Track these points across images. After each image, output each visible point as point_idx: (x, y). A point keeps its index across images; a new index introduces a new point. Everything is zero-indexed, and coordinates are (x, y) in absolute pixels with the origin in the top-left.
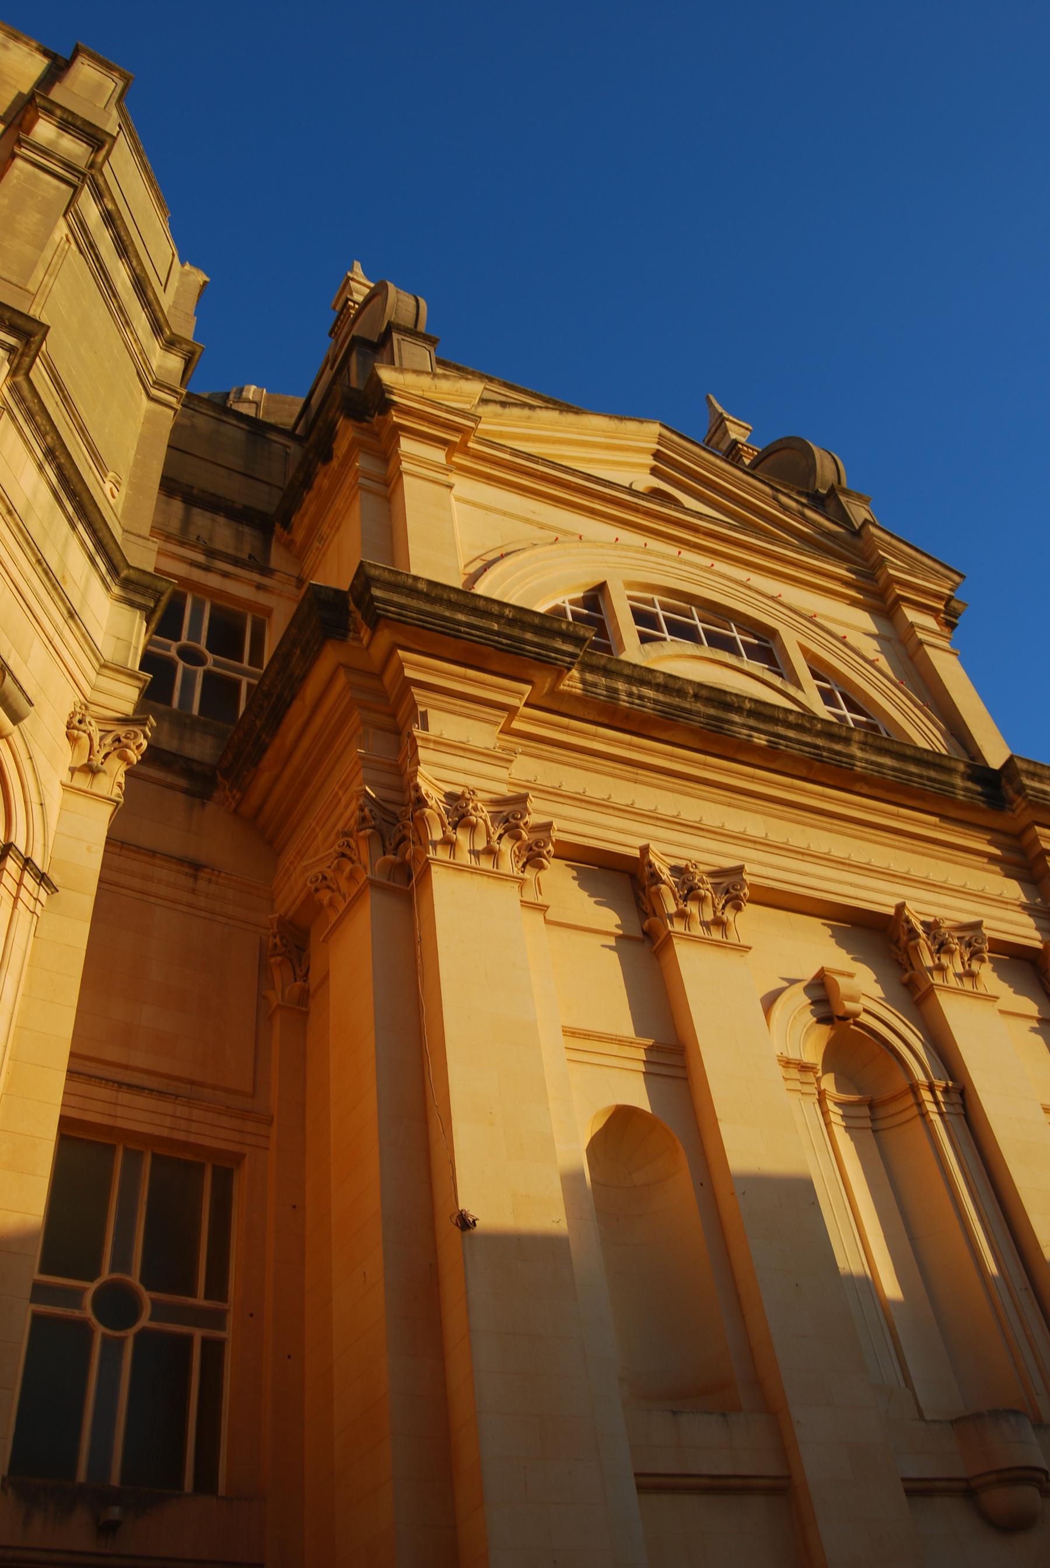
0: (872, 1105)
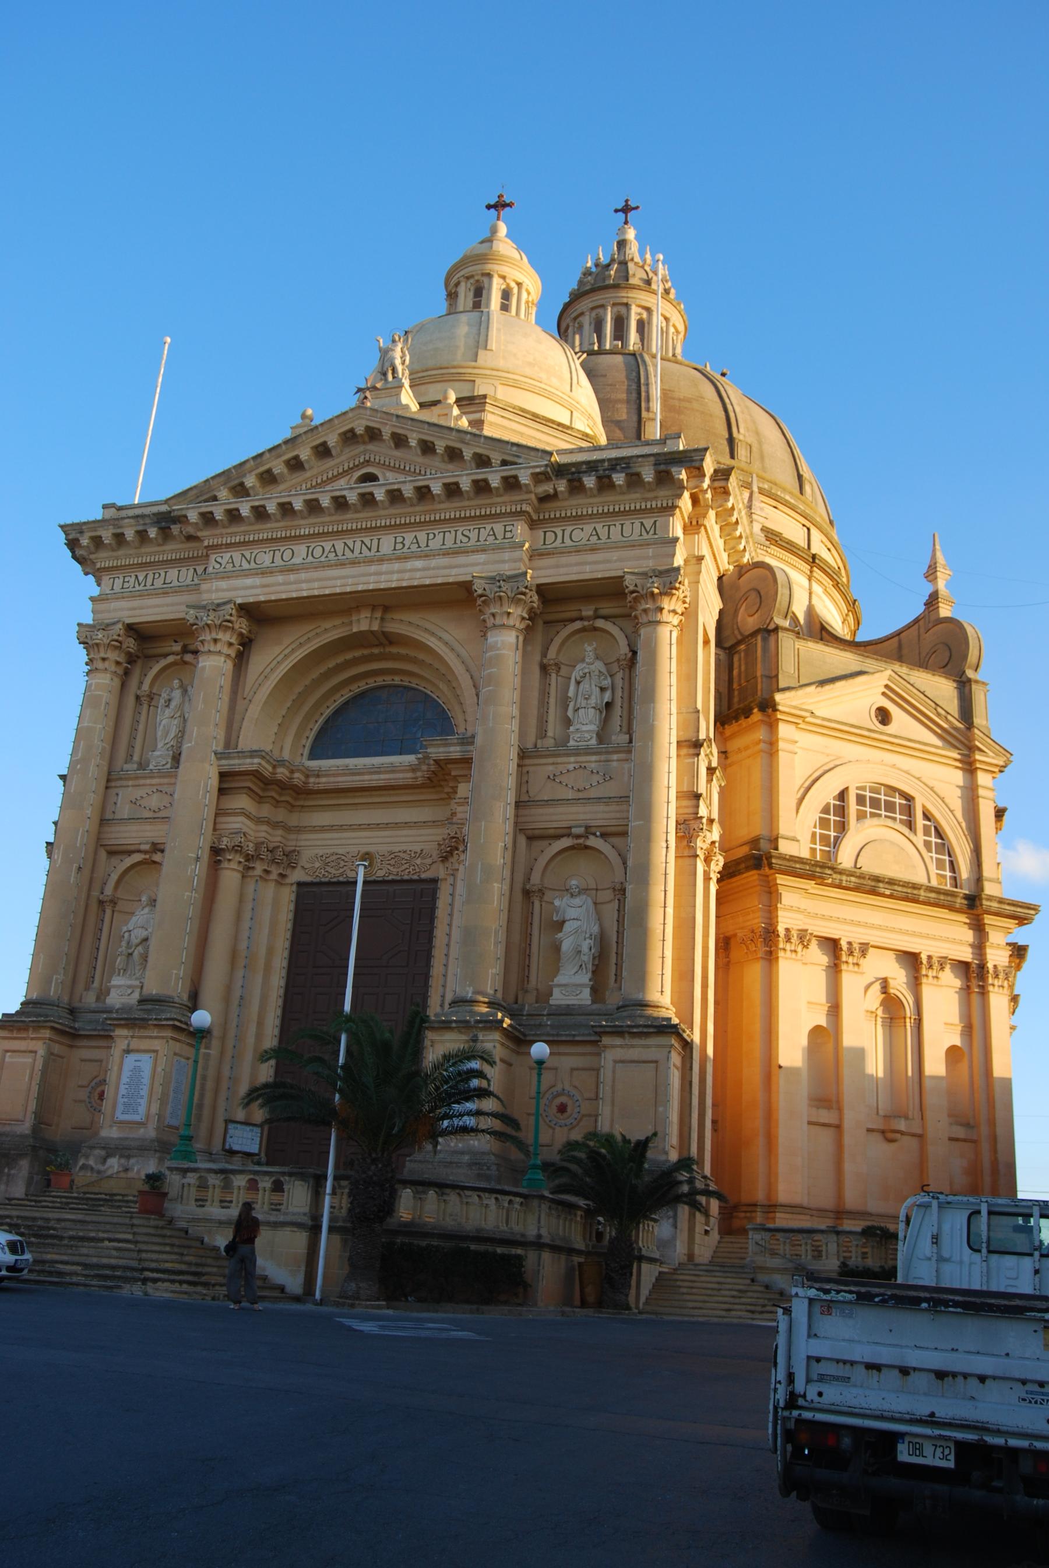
0: (891, 1019)
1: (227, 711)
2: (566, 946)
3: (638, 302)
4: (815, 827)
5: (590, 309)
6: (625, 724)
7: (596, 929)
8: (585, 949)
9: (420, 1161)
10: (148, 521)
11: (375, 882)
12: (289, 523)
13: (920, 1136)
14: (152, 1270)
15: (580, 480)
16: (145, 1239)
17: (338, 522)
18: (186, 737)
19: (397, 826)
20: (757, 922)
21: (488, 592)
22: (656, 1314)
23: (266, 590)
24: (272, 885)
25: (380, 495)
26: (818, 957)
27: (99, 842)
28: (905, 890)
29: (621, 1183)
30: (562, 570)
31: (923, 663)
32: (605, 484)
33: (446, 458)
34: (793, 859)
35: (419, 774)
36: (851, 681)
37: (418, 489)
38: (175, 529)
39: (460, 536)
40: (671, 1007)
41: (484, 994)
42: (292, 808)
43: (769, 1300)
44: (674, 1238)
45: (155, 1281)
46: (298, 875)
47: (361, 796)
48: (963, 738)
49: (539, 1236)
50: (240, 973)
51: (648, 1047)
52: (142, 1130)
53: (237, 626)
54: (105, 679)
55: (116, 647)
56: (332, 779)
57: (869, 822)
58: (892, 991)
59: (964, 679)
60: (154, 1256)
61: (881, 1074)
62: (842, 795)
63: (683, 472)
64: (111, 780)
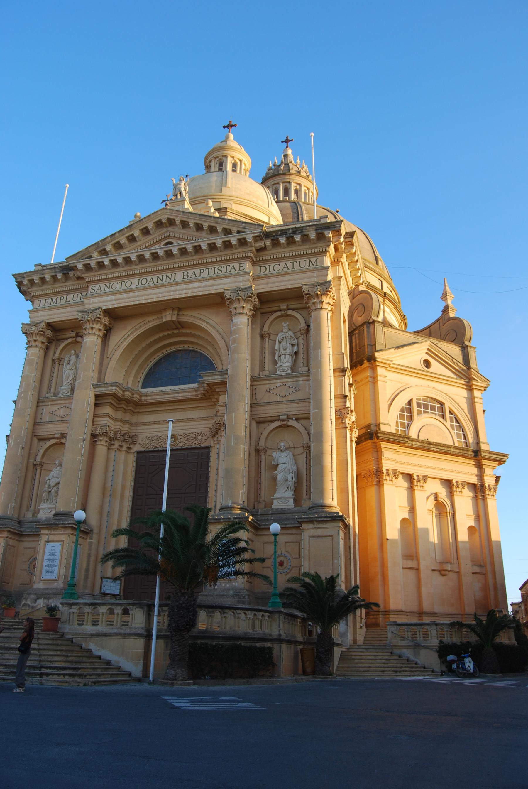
1: (97, 364)
2: (280, 478)
3: (295, 181)
4: (397, 419)
5: (274, 179)
6: (305, 362)
7: (295, 468)
8: (290, 478)
9: (206, 595)
10: (57, 270)
11: (177, 450)
12: (129, 268)
13: (458, 572)
14: (47, 668)
15: (277, 239)
16: (46, 647)
17: (154, 266)
18: (78, 377)
19: (188, 420)
20: (372, 466)
21: (232, 297)
22: (345, 675)
23: (118, 302)
24: (124, 453)
25: (175, 251)
26: (403, 483)
27: (33, 434)
28: (444, 448)
29: (322, 602)
30: (270, 285)
31: (443, 338)
32: (290, 241)
33: (209, 232)
34: (389, 434)
35: (199, 393)
36: (411, 347)
37: (195, 247)
38: (71, 274)
39: (217, 270)
40: (337, 507)
41: (238, 504)
42: (133, 413)
43: (403, 664)
44: (347, 631)
45: (48, 675)
46: (137, 448)
47: (170, 406)
48: (466, 374)
49: (280, 635)
50: (107, 499)
51: (327, 528)
52: (56, 584)
53: (103, 321)
54: (37, 352)
55: (41, 335)
56: (154, 397)
57: (423, 415)
58: (440, 499)
59: (464, 345)
60: (49, 658)
61: (436, 541)
62: (410, 403)
63: (331, 233)
64: (39, 402)
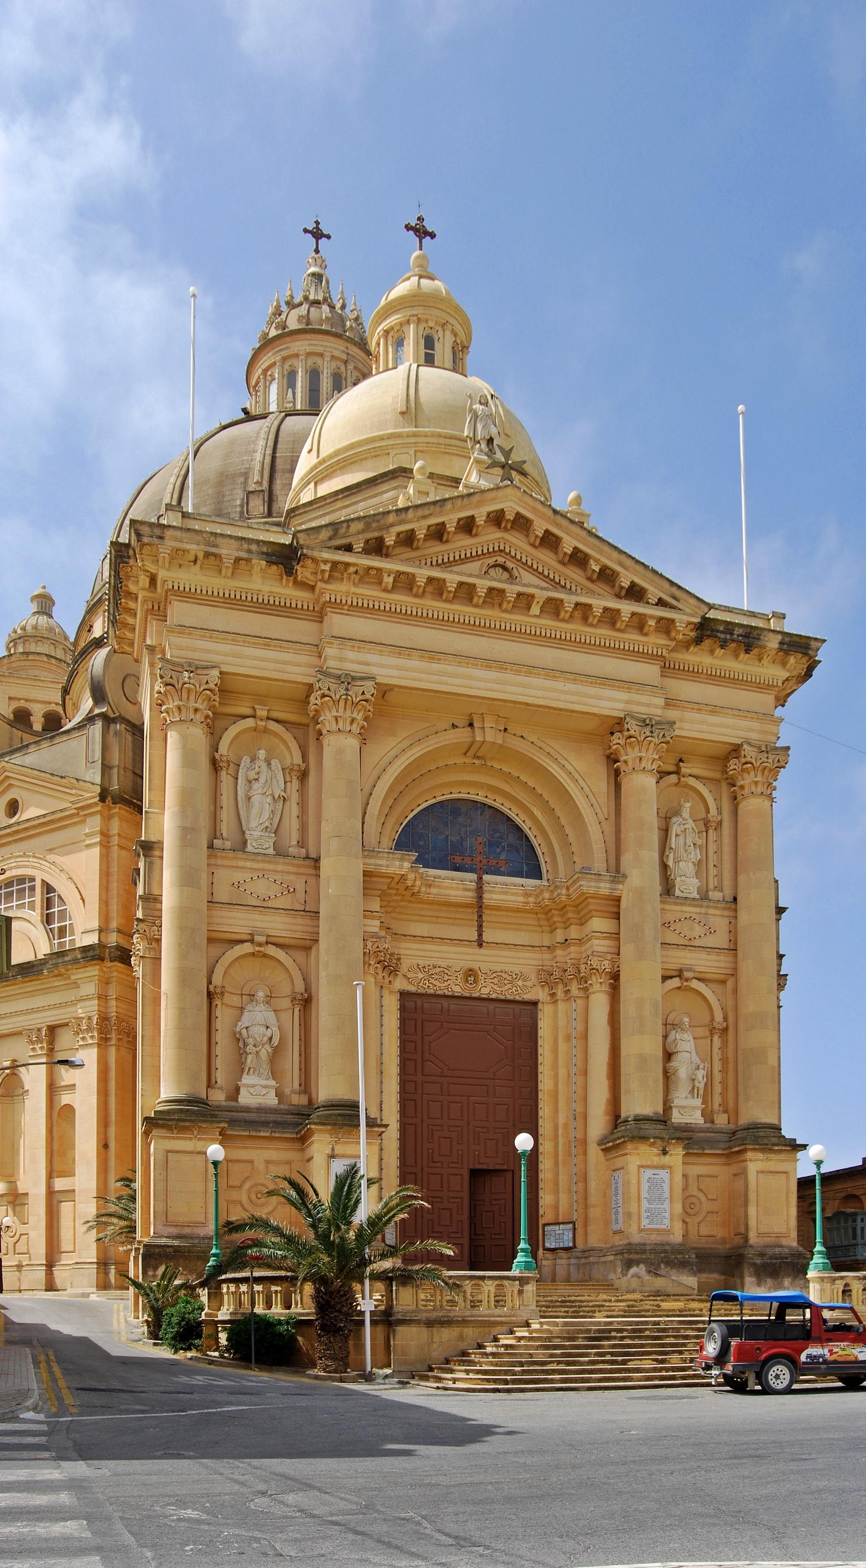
35: (531, 899)
